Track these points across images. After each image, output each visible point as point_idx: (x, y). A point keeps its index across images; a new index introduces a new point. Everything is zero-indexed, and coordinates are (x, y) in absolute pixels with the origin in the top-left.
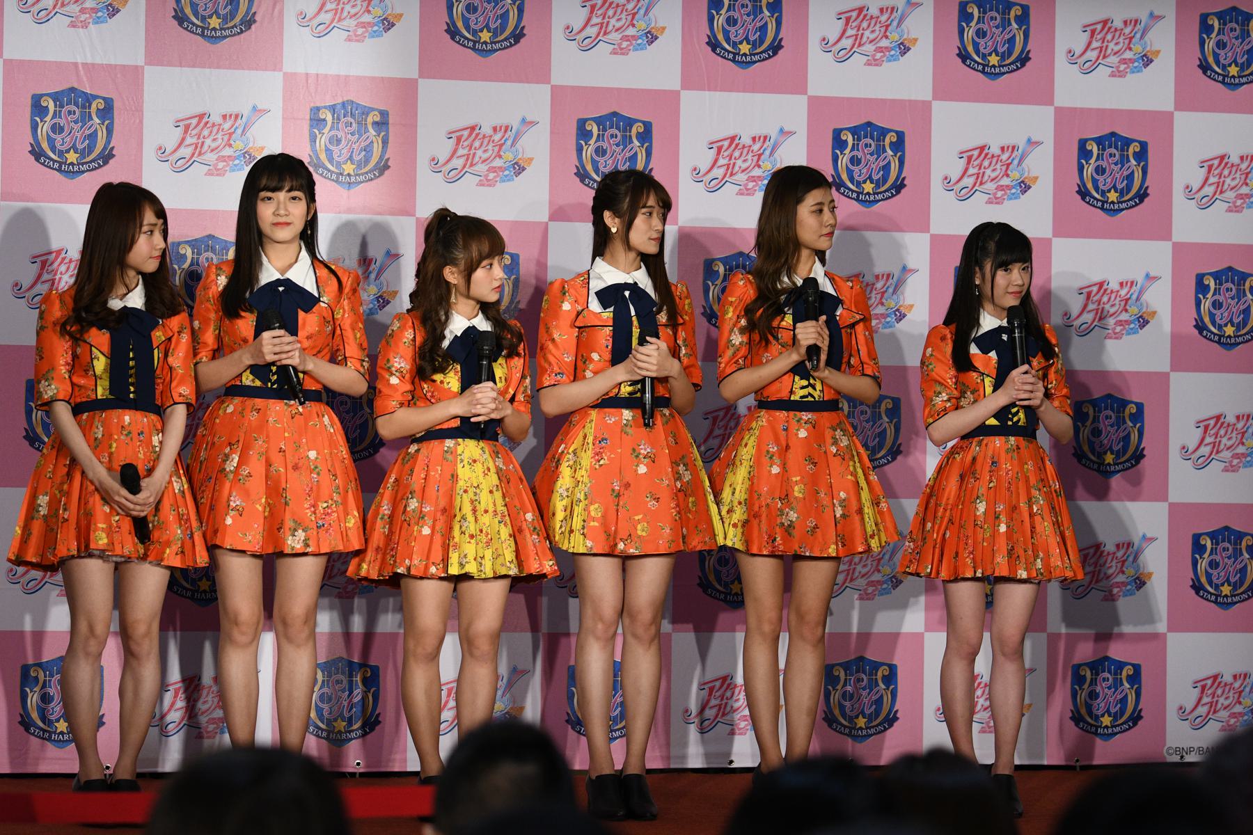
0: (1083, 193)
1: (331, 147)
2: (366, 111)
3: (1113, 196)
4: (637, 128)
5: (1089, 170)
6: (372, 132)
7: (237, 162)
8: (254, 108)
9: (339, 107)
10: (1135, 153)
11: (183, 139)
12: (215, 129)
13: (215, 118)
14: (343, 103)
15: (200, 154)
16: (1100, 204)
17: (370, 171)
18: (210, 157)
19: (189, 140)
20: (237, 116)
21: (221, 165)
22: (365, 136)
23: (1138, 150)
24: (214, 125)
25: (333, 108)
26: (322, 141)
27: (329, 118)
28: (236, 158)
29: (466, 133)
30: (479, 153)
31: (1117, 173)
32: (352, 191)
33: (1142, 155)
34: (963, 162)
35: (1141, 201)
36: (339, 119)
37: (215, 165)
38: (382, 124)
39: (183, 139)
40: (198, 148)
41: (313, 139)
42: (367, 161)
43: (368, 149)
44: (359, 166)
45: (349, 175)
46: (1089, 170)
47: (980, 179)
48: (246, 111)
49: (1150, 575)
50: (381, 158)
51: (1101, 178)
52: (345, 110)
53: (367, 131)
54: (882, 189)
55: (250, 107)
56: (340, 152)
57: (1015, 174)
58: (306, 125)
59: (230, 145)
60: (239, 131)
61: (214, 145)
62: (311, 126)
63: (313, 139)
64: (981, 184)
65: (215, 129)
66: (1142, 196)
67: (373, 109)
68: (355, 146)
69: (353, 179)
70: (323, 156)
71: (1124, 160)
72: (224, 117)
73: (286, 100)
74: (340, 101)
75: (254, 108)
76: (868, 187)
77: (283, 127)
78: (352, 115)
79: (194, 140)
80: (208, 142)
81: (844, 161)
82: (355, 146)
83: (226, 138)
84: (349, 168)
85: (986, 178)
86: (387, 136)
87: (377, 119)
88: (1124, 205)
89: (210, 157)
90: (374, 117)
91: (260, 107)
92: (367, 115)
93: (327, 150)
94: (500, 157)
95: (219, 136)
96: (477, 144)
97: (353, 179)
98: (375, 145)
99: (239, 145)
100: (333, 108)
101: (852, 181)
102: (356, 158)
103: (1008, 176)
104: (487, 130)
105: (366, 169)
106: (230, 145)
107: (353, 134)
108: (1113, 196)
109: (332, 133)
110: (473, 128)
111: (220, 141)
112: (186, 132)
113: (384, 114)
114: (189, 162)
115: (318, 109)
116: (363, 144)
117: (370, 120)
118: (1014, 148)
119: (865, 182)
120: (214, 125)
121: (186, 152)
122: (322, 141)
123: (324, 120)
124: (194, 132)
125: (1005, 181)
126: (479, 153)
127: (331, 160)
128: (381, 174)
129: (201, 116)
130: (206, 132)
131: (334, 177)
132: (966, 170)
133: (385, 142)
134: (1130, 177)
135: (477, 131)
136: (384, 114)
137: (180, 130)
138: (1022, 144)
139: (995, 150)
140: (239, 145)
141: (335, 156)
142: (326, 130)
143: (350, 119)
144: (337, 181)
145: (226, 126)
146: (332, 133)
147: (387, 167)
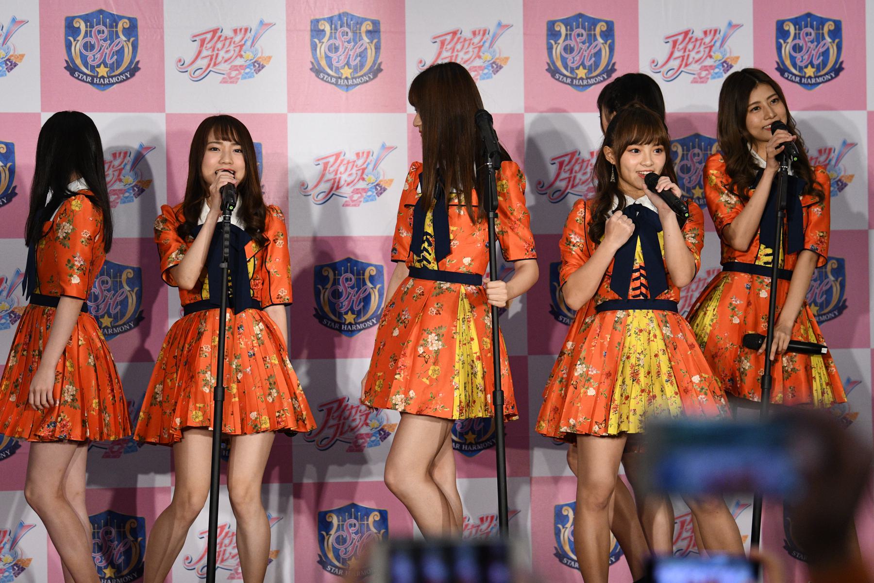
0: (72, 69)
1: (330, 54)
2: (360, 22)
3: (103, 71)
4: (123, 24)
5: (558, 49)
6: (366, 39)
7: (247, 70)
8: (262, 23)
9: (335, 19)
10: (830, 31)
11: (200, 52)
12: (228, 42)
13: (228, 32)
14: (340, 15)
15: (215, 65)
16: (569, 81)
17: (365, 75)
18: (224, 67)
19: (205, 53)
20: (246, 30)
21: (234, 74)
22: (359, 44)
23: (832, 28)
24: (226, 39)
25: (330, 20)
26: (322, 49)
27: (327, 28)
28: (247, 67)
29: (449, 37)
30: (461, 54)
31: (814, 51)
32: (351, 92)
33: (836, 33)
34: (669, 46)
35: (837, 75)
36: (336, 29)
37: (229, 74)
38: (375, 33)
39: (200, 52)
40: (213, 60)
41: (314, 47)
42: (362, 66)
43: (362, 55)
44: (355, 70)
45: (347, 78)
46: (787, 49)
47: (685, 61)
48: (254, 25)
49: (857, 414)
50: (374, 63)
51: (798, 56)
52: (340, 21)
53: (361, 39)
54: (594, 74)
55: (258, 22)
56: (338, 59)
57: (717, 55)
58: (307, 36)
59: (241, 56)
60: (249, 43)
61: (227, 56)
62: (312, 37)
63: (314, 47)
64: (686, 65)
65: (228, 42)
66: (837, 70)
67: (366, 20)
68: (351, 53)
69: (350, 82)
70: (323, 63)
71: (820, 38)
72: (235, 31)
73: (288, 16)
74: (336, 13)
75: (262, 23)
76: (103, 71)
77: (289, 38)
78: (348, 26)
79: (209, 53)
80: (222, 53)
81: (558, 49)
82: (351, 53)
83: (237, 49)
84: (346, 72)
85: (690, 60)
86: (379, 42)
87: (370, 28)
88: (821, 79)
89: (224, 67)
90: (367, 26)
91: (266, 21)
92: (361, 24)
93: (327, 57)
94: (479, 57)
95: (232, 48)
96: (459, 46)
97: (350, 82)
98: (369, 51)
99: (248, 55)
100: (330, 20)
101: (566, 68)
102: (353, 63)
103: (711, 57)
104: (467, 34)
105: (362, 73)
106: (241, 56)
107: (349, 42)
108: (810, 72)
109: (331, 41)
110: (455, 33)
111: (232, 52)
112: (202, 45)
113: (376, 23)
114: (206, 72)
115: (318, 21)
116: (359, 51)
117: (364, 29)
118: (716, 31)
119: (578, 68)
120: (226, 39)
121: (202, 63)
122: (322, 49)
123: (323, 30)
124: (209, 46)
125: (709, 62)
126: (461, 54)
127: (330, 66)
128: (375, 76)
129: (215, 31)
130: (219, 45)
131: (334, 80)
132: (672, 54)
133: (378, 48)
134: (826, 54)
135: (458, 35)
136: (376, 23)
137: (197, 44)
138: (723, 27)
139: (699, 34)
140: (248, 55)
141: (334, 63)
142: (325, 40)
143: (346, 29)
144: (336, 84)
145: (237, 39)
146: (331, 41)
147: (380, 70)
